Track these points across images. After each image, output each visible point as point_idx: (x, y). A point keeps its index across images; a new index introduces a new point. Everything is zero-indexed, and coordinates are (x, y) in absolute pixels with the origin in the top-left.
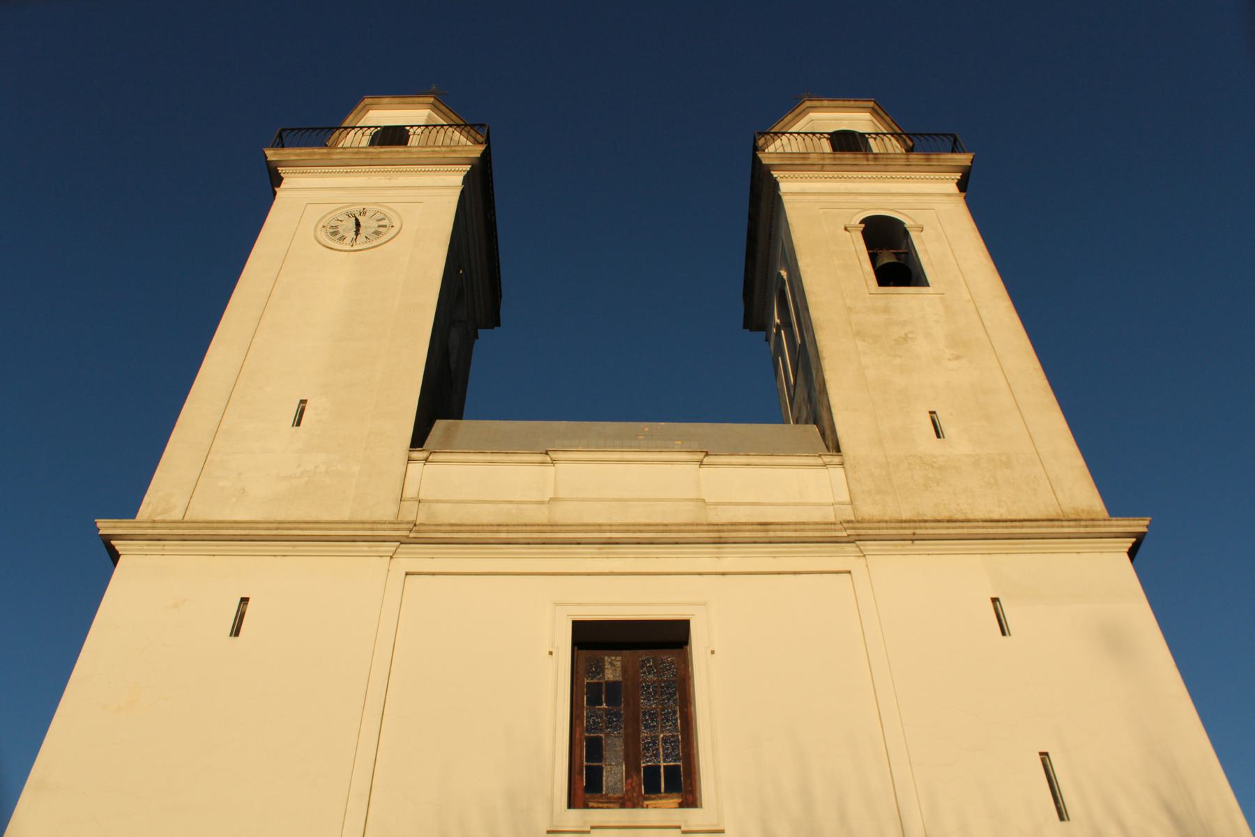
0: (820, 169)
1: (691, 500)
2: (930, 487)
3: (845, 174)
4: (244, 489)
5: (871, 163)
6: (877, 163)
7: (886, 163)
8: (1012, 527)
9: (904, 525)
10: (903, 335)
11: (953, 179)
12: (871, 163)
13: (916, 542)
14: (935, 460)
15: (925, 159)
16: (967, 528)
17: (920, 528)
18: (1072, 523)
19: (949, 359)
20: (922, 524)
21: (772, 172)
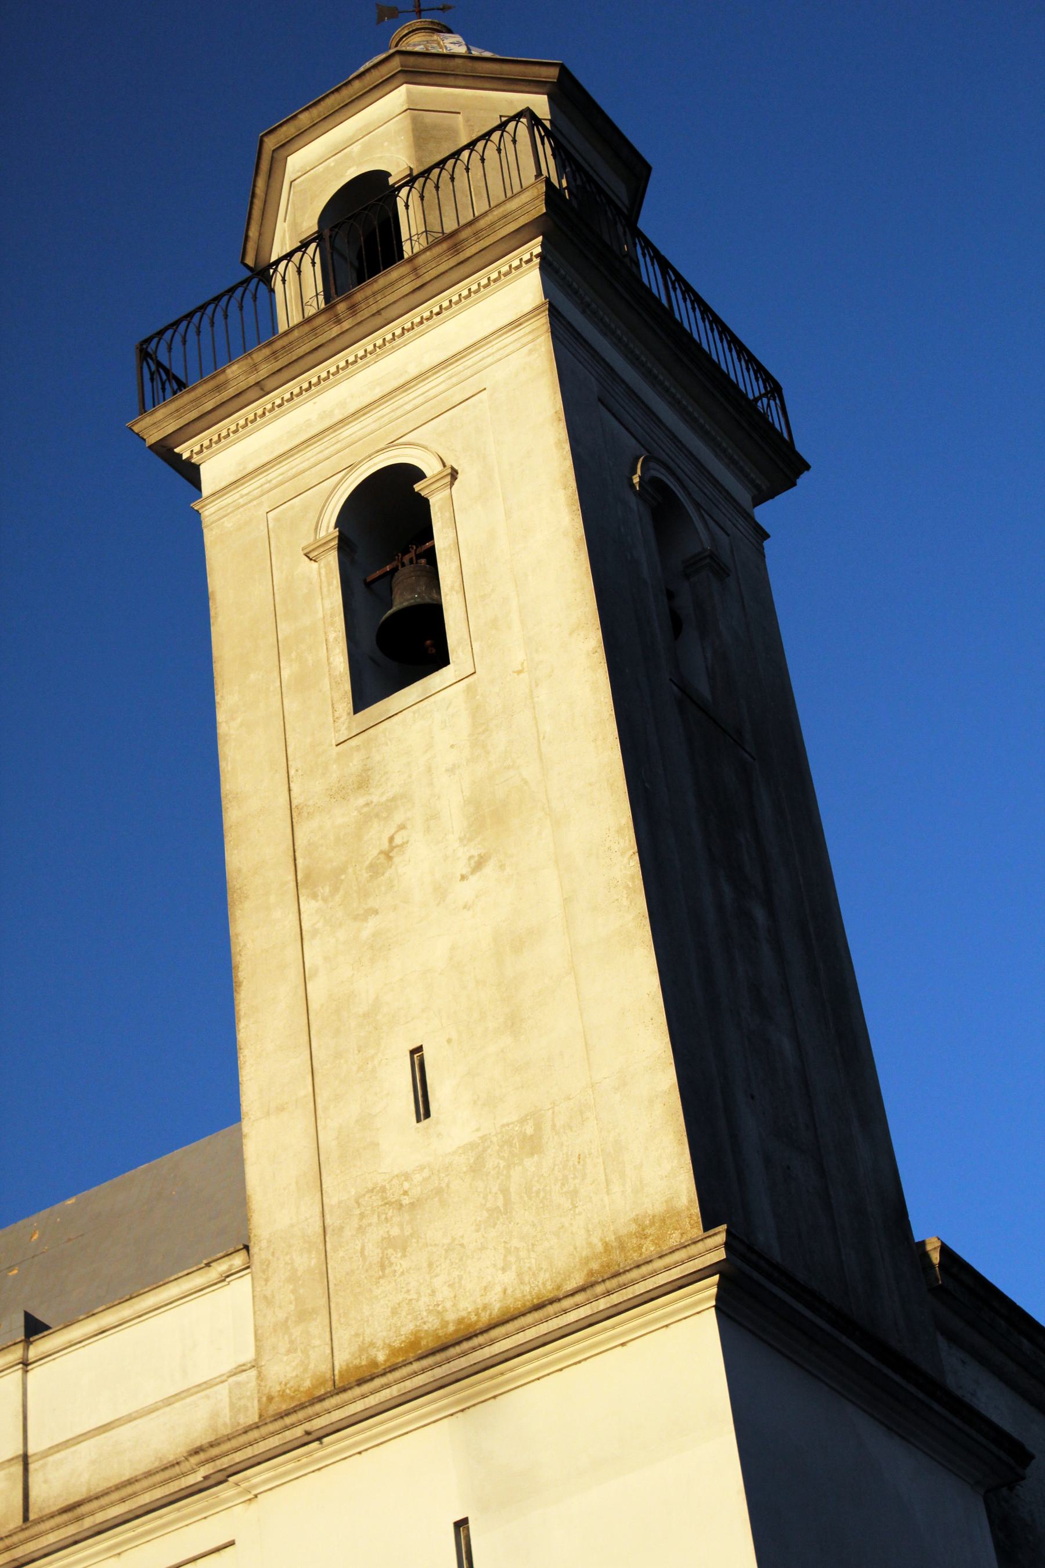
0: (262, 393)
2: (391, 1264)
3: (312, 376)
5: (346, 325)
6: (359, 318)
7: (374, 309)
8: (474, 1349)
9: (288, 1420)
10: (385, 846)
11: (528, 261)
12: (346, 325)
13: (326, 1440)
14: (406, 1186)
15: (449, 249)
16: (397, 1382)
17: (318, 1415)
18: (579, 1298)
19: (463, 878)
20: (318, 1407)
21: (177, 450)
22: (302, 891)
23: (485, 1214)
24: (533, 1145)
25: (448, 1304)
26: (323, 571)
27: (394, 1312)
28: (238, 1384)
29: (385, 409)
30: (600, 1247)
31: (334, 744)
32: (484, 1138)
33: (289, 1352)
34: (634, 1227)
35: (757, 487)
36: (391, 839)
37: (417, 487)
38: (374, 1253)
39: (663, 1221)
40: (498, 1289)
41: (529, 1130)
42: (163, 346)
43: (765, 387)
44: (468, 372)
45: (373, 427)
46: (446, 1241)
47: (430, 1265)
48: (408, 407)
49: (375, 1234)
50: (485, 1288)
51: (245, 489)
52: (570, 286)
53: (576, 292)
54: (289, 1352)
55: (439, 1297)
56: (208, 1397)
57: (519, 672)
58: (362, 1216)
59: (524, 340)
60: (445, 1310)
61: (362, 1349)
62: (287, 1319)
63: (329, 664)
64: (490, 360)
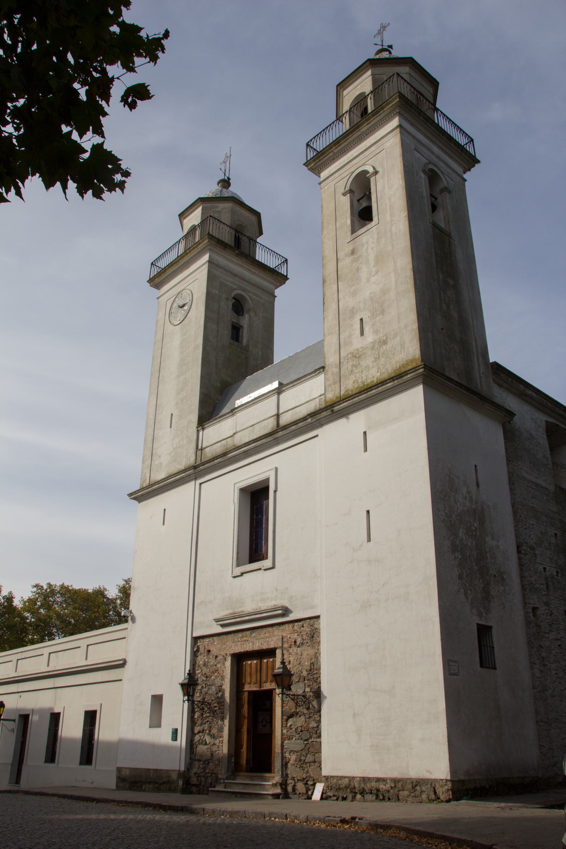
1: (272, 416)
4: (161, 463)
22: (339, 280)
23: (374, 359)
24: (385, 342)
25: (365, 381)
26: (346, 199)
27: (354, 383)
28: (321, 399)
29: (362, 156)
30: (398, 367)
31: (347, 242)
32: (374, 341)
33: (331, 391)
34: (406, 363)
35: (465, 168)
36: (358, 266)
37: (368, 176)
38: (350, 368)
39: (412, 361)
40: (376, 377)
41: (385, 338)
42: (312, 143)
43: (468, 140)
44: (381, 145)
45: (359, 160)
46: (366, 365)
47: (362, 371)
48: (367, 155)
49: (351, 364)
50: (373, 377)
51: (330, 179)
52: (407, 119)
53: (409, 121)
54: (331, 391)
55: (363, 379)
56: (314, 401)
57: (388, 223)
58: (348, 359)
59: (394, 135)
60: (364, 382)
61: (346, 391)
62: (331, 384)
63: (346, 222)
64: (386, 141)
